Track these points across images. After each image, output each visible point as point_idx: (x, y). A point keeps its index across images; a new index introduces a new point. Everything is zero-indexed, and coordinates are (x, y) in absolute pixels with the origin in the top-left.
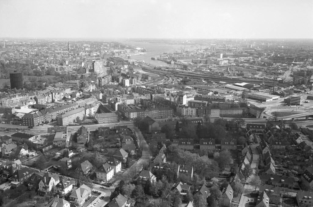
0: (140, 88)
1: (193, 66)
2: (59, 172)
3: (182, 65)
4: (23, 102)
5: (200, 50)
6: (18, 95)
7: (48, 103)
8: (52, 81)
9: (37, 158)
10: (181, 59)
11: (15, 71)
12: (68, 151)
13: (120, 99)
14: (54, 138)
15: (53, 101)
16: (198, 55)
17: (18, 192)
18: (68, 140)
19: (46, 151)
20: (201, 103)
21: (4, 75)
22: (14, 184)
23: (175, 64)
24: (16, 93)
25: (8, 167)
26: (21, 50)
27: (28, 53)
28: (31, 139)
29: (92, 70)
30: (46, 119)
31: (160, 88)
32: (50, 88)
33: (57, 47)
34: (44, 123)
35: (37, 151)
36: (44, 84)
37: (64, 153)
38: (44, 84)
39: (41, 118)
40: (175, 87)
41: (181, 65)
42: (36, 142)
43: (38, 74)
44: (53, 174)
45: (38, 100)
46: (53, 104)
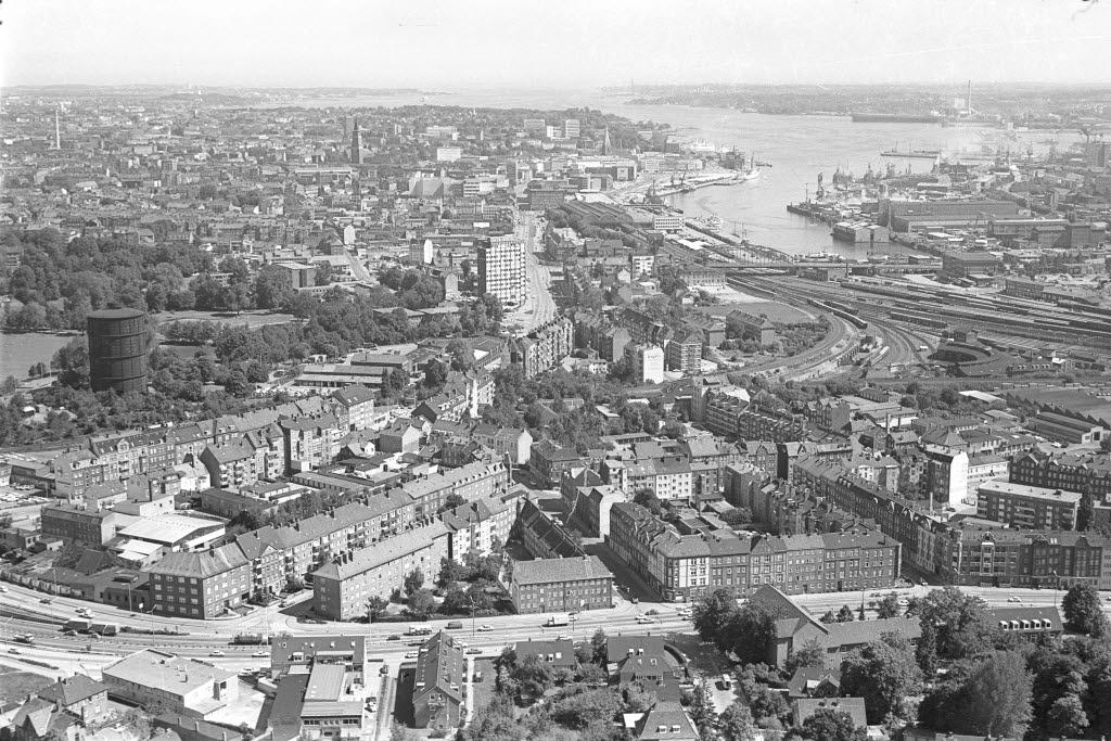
0: (725, 398)
4: (153, 483)
6: (126, 439)
13: (620, 472)
14: (303, 700)
15: (291, 472)
20: (1046, 502)
29: (473, 284)
30: (260, 581)
31: (824, 401)
34: (250, 602)
45: (223, 468)
46: (294, 487)
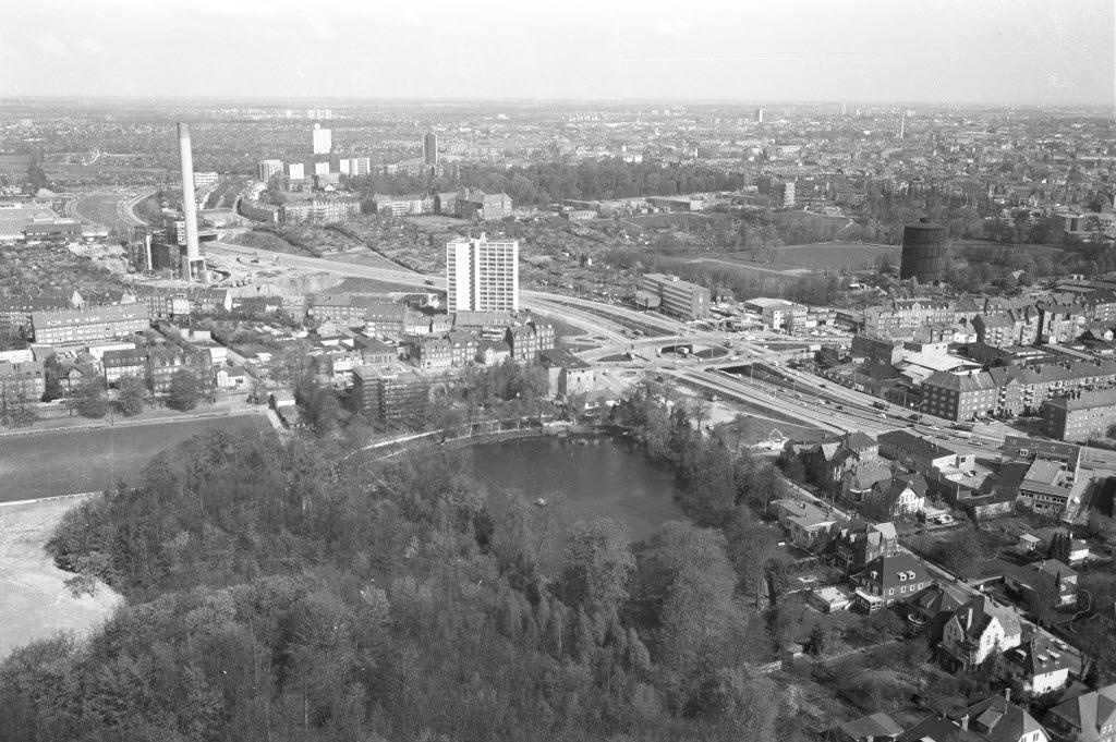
2: (1023, 609)
4: (935, 330)
6: (920, 302)
7: (1020, 345)
8: (1050, 266)
9: (951, 533)
11: (923, 220)
12: (1068, 538)
15: (1040, 342)
17: (871, 630)
18: (1077, 500)
19: (985, 519)
21: (885, 229)
22: (865, 600)
24: (913, 296)
25: (853, 537)
26: (952, 149)
27: (976, 160)
28: (942, 463)
30: (1003, 404)
32: (1035, 292)
33: (1086, 140)
34: (993, 417)
35: (953, 508)
36: (1016, 274)
37: (1053, 542)
38: (1016, 274)
39: (986, 396)
42: (956, 478)
43: (999, 238)
44: (1001, 606)
45: (988, 330)
46: (1040, 352)
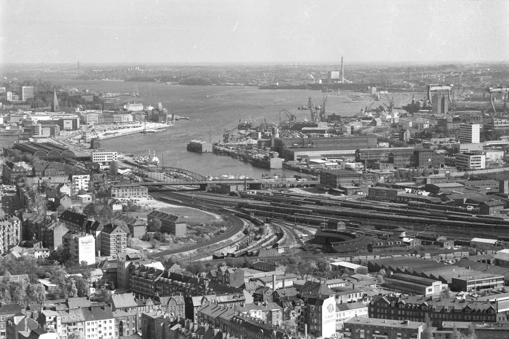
1: (360, 175)
3: (317, 174)
5: (390, 111)
10: (311, 149)
16: (379, 130)
23: (286, 167)
40: (289, 262)
41: (312, 172)
